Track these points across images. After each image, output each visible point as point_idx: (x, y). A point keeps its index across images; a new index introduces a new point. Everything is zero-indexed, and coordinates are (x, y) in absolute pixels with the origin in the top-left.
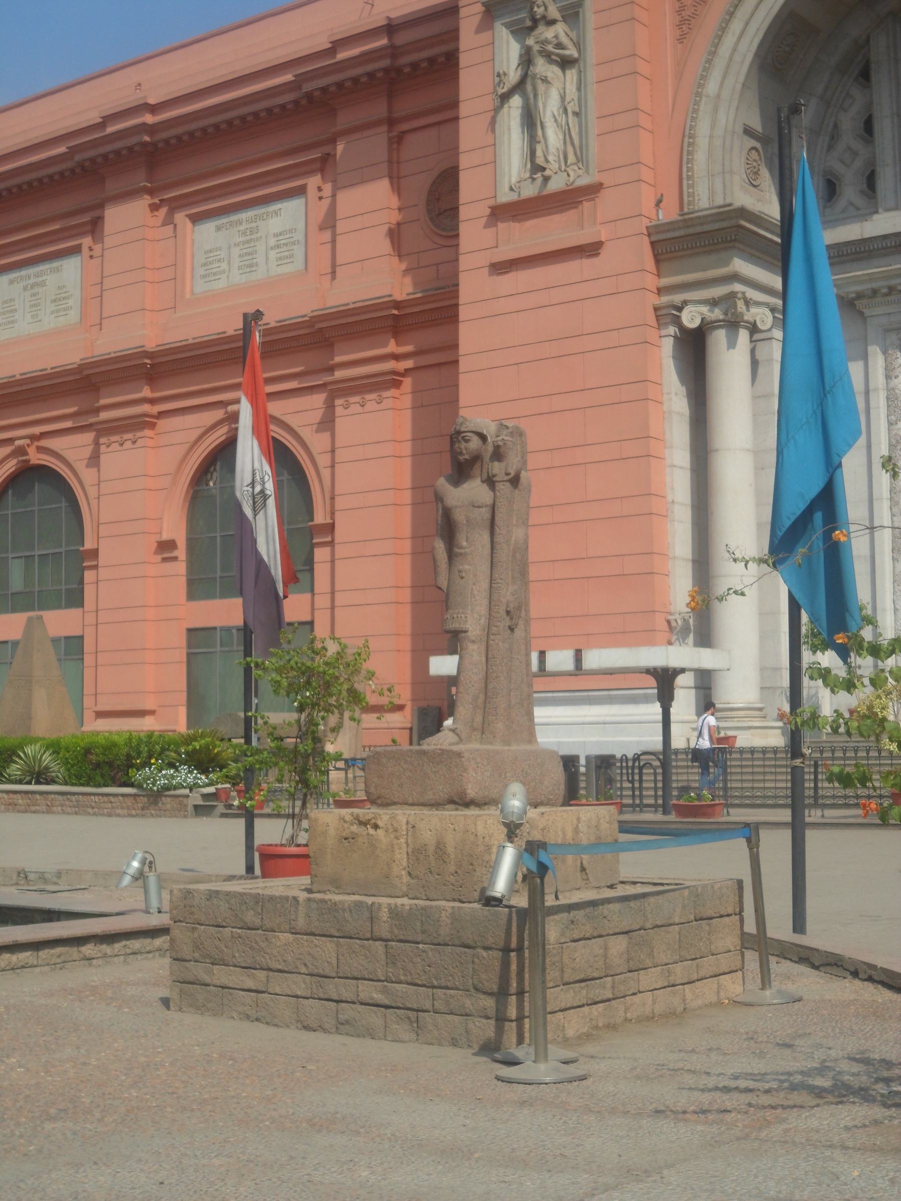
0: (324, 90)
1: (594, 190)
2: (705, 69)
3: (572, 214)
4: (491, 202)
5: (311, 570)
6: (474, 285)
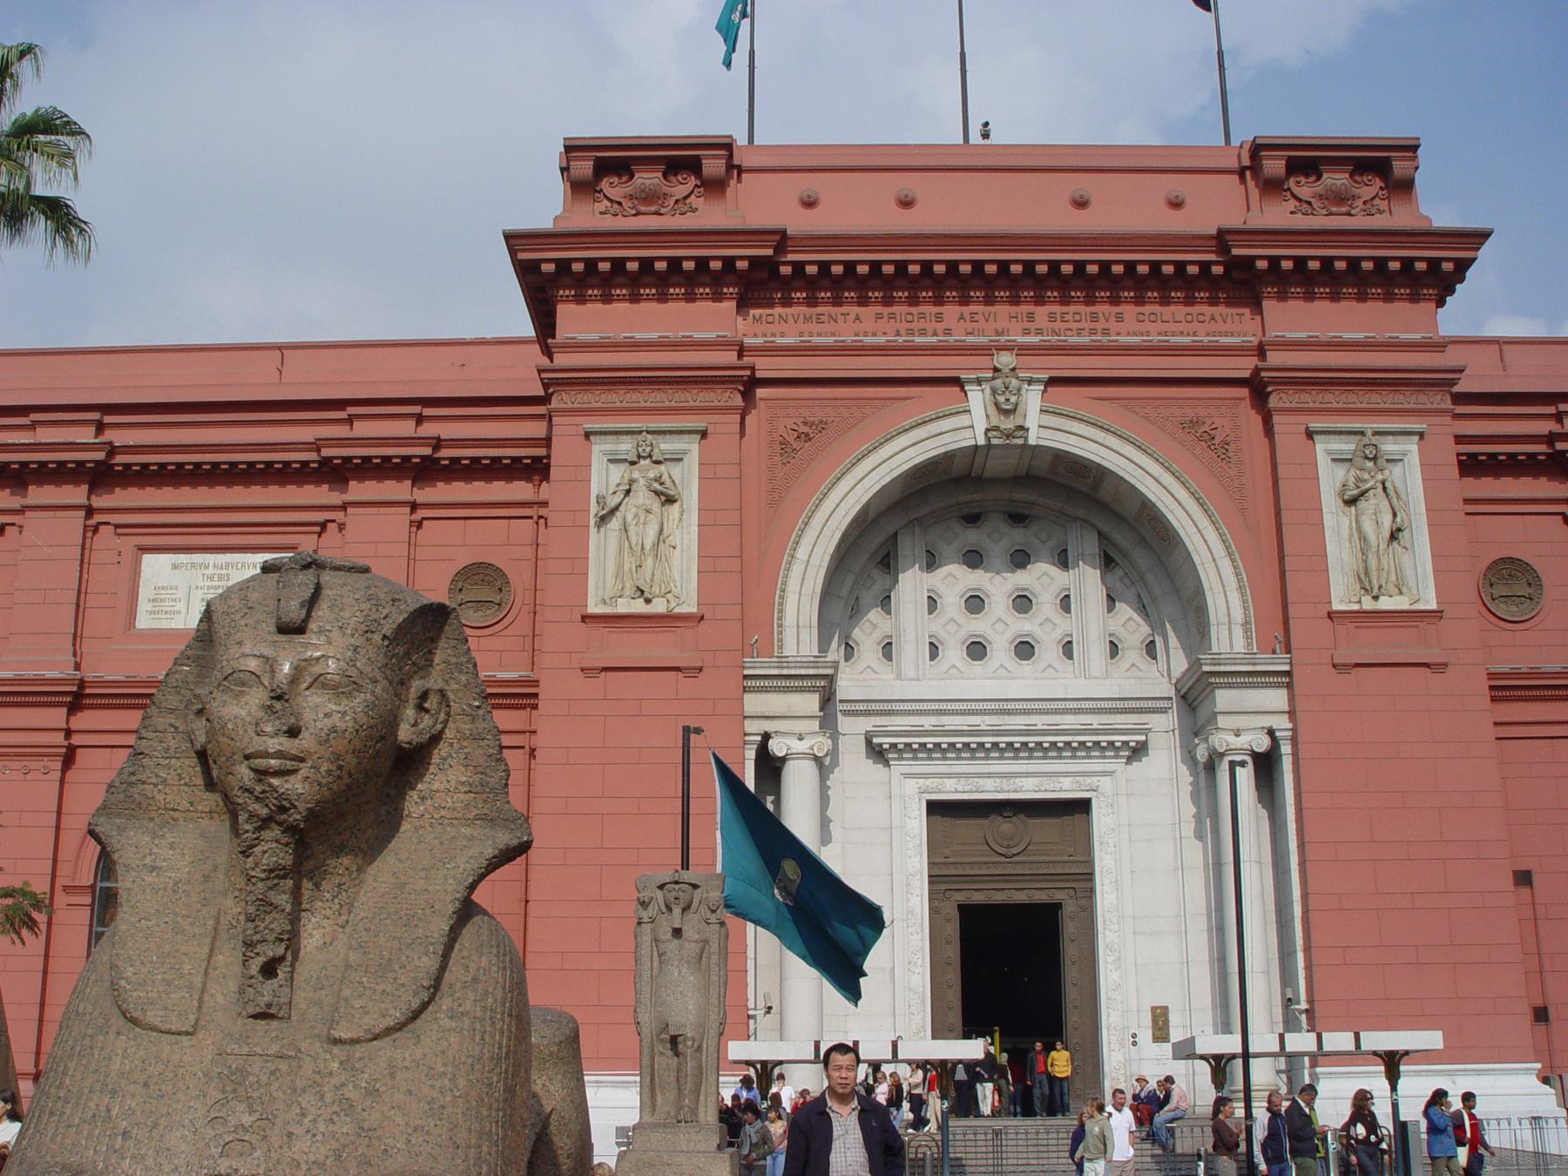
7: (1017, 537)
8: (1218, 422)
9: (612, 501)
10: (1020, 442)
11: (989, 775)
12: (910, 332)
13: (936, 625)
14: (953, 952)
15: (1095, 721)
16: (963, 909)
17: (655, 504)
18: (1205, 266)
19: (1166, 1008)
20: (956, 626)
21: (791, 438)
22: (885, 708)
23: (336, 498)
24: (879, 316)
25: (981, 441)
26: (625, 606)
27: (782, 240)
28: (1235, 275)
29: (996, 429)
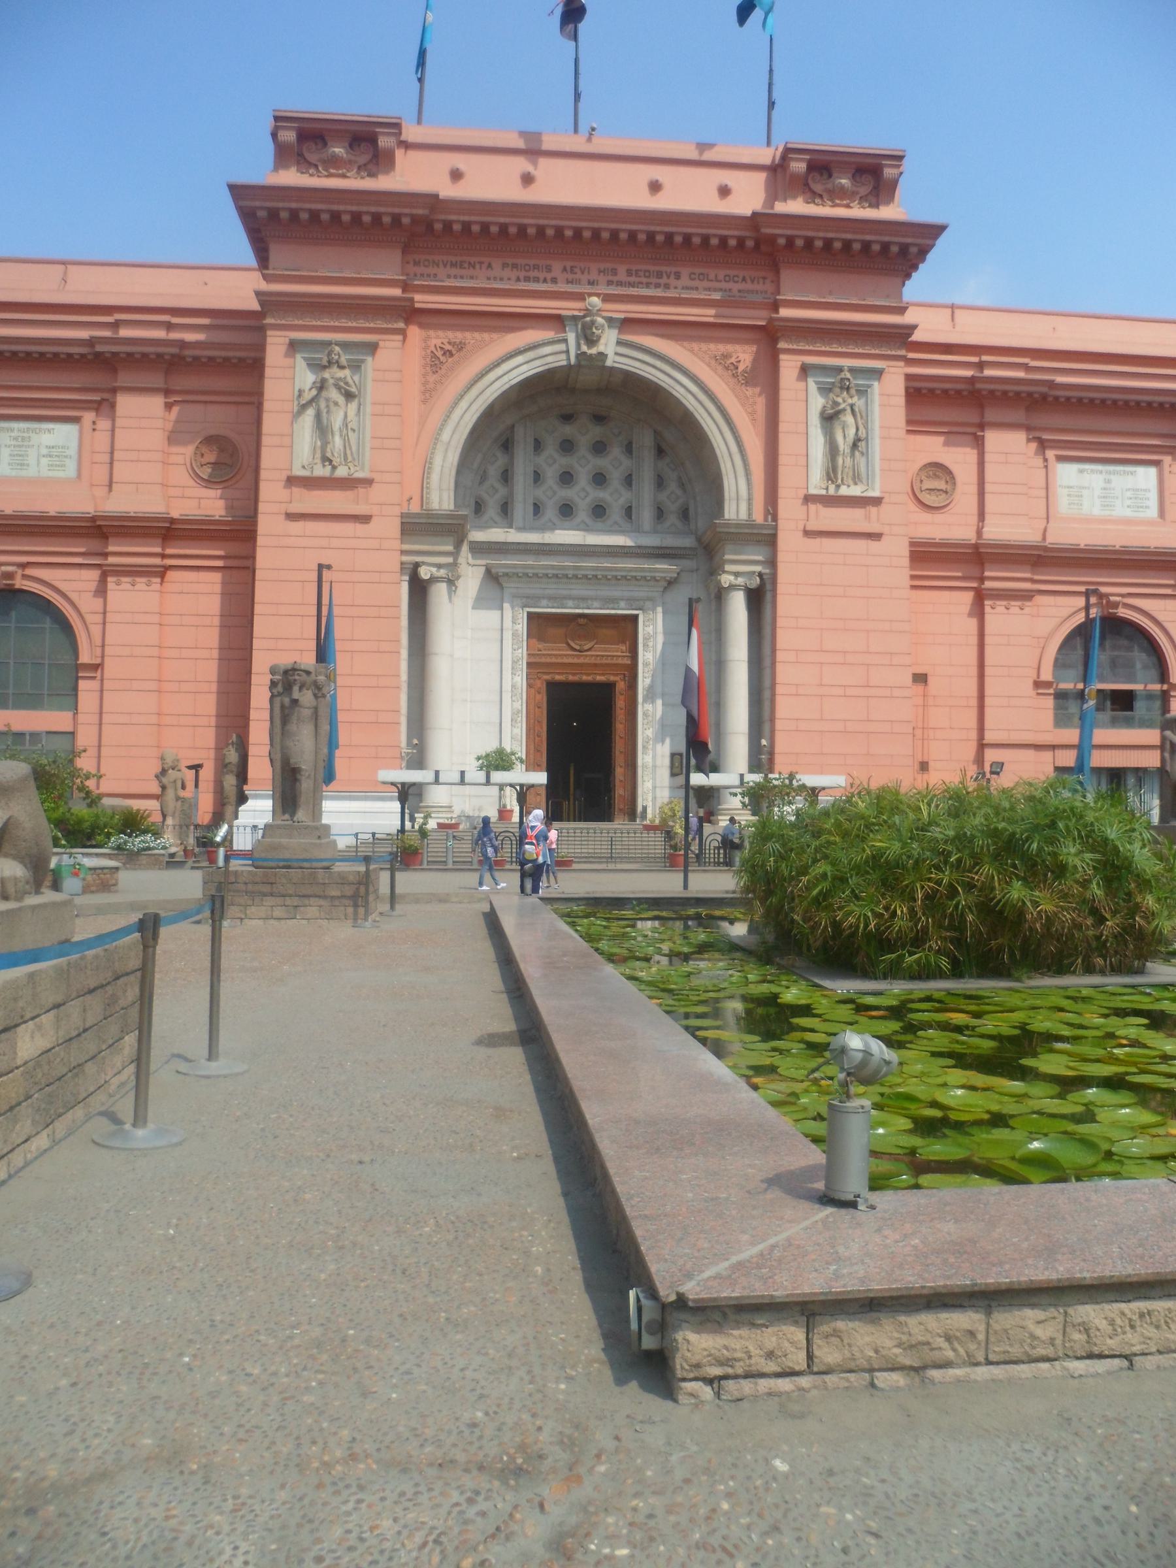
0: (115, 354)
1: (368, 482)
2: (443, 425)
3: (349, 493)
4: (289, 473)
5: (76, 695)
6: (268, 524)
8: (742, 356)
9: (308, 396)
10: (600, 364)
11: (570, 598)
12: (527, 279)
13: (539, 492)
16: (552, 687)
17: (341, 400)
18: (741, 241)
20: (552, 493)
21: (439, 353)
24: (505, 265)
26: (321, 471)
28: (763, 248)
29: (585, 353)
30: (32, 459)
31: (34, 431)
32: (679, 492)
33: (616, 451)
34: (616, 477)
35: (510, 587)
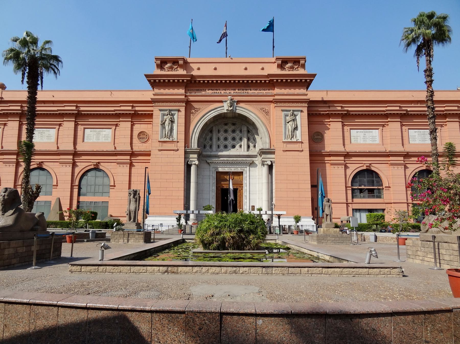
7: (233, 127)
13: (219, 143)
14: (220, 195)
15: (244, 159)
19: (254, 206)
20: (222, 143)
22: (210, 156)
23: (118, 120)
24: (209, 90)
25: (226, 111)
27: (192, 76)
28: (271, 82)
30: (101, 138)
31: (101, 131)
32: (253, 141)
33: (238, 132)
34: (237, 138)
35: (212, 165)
